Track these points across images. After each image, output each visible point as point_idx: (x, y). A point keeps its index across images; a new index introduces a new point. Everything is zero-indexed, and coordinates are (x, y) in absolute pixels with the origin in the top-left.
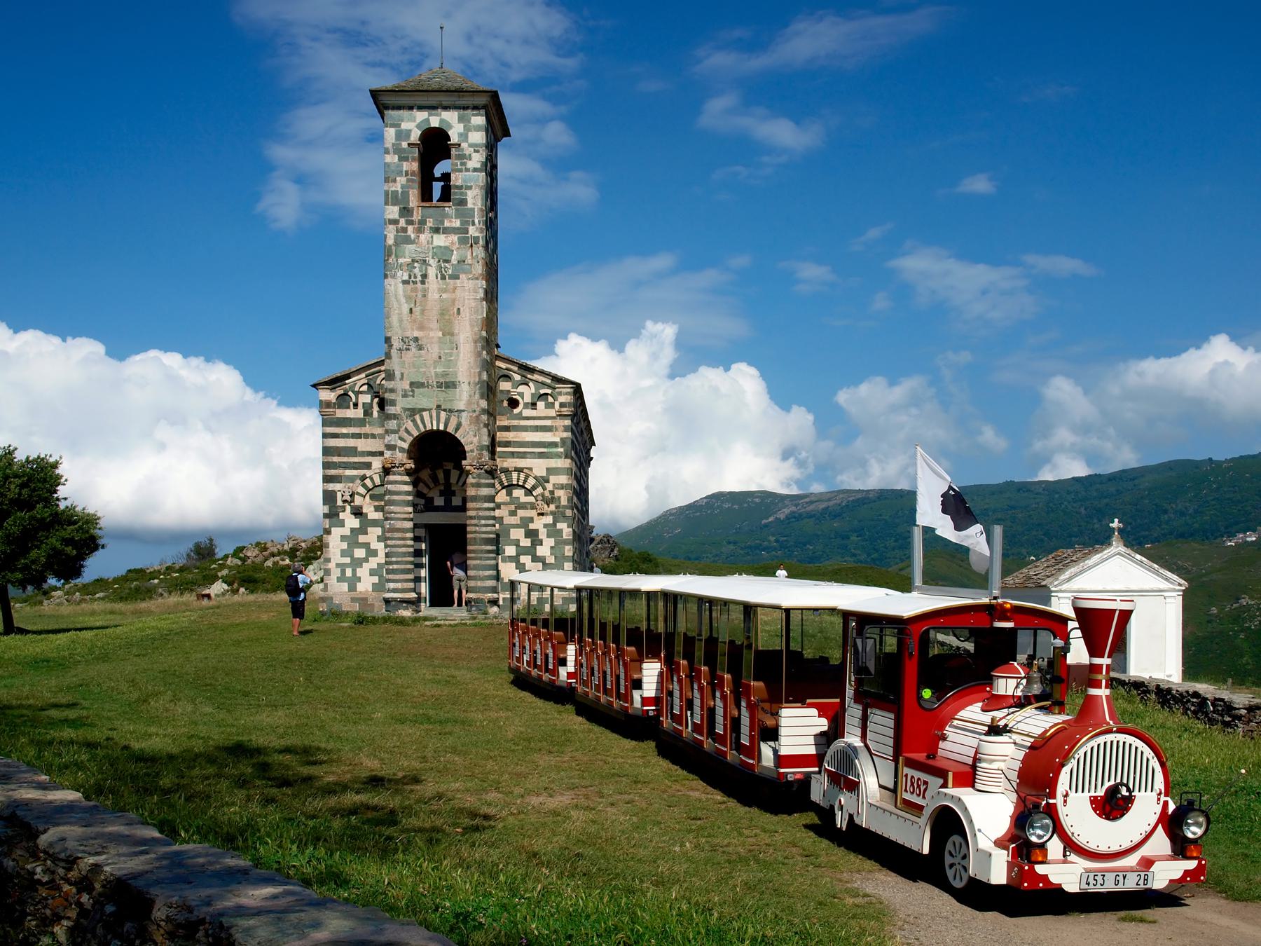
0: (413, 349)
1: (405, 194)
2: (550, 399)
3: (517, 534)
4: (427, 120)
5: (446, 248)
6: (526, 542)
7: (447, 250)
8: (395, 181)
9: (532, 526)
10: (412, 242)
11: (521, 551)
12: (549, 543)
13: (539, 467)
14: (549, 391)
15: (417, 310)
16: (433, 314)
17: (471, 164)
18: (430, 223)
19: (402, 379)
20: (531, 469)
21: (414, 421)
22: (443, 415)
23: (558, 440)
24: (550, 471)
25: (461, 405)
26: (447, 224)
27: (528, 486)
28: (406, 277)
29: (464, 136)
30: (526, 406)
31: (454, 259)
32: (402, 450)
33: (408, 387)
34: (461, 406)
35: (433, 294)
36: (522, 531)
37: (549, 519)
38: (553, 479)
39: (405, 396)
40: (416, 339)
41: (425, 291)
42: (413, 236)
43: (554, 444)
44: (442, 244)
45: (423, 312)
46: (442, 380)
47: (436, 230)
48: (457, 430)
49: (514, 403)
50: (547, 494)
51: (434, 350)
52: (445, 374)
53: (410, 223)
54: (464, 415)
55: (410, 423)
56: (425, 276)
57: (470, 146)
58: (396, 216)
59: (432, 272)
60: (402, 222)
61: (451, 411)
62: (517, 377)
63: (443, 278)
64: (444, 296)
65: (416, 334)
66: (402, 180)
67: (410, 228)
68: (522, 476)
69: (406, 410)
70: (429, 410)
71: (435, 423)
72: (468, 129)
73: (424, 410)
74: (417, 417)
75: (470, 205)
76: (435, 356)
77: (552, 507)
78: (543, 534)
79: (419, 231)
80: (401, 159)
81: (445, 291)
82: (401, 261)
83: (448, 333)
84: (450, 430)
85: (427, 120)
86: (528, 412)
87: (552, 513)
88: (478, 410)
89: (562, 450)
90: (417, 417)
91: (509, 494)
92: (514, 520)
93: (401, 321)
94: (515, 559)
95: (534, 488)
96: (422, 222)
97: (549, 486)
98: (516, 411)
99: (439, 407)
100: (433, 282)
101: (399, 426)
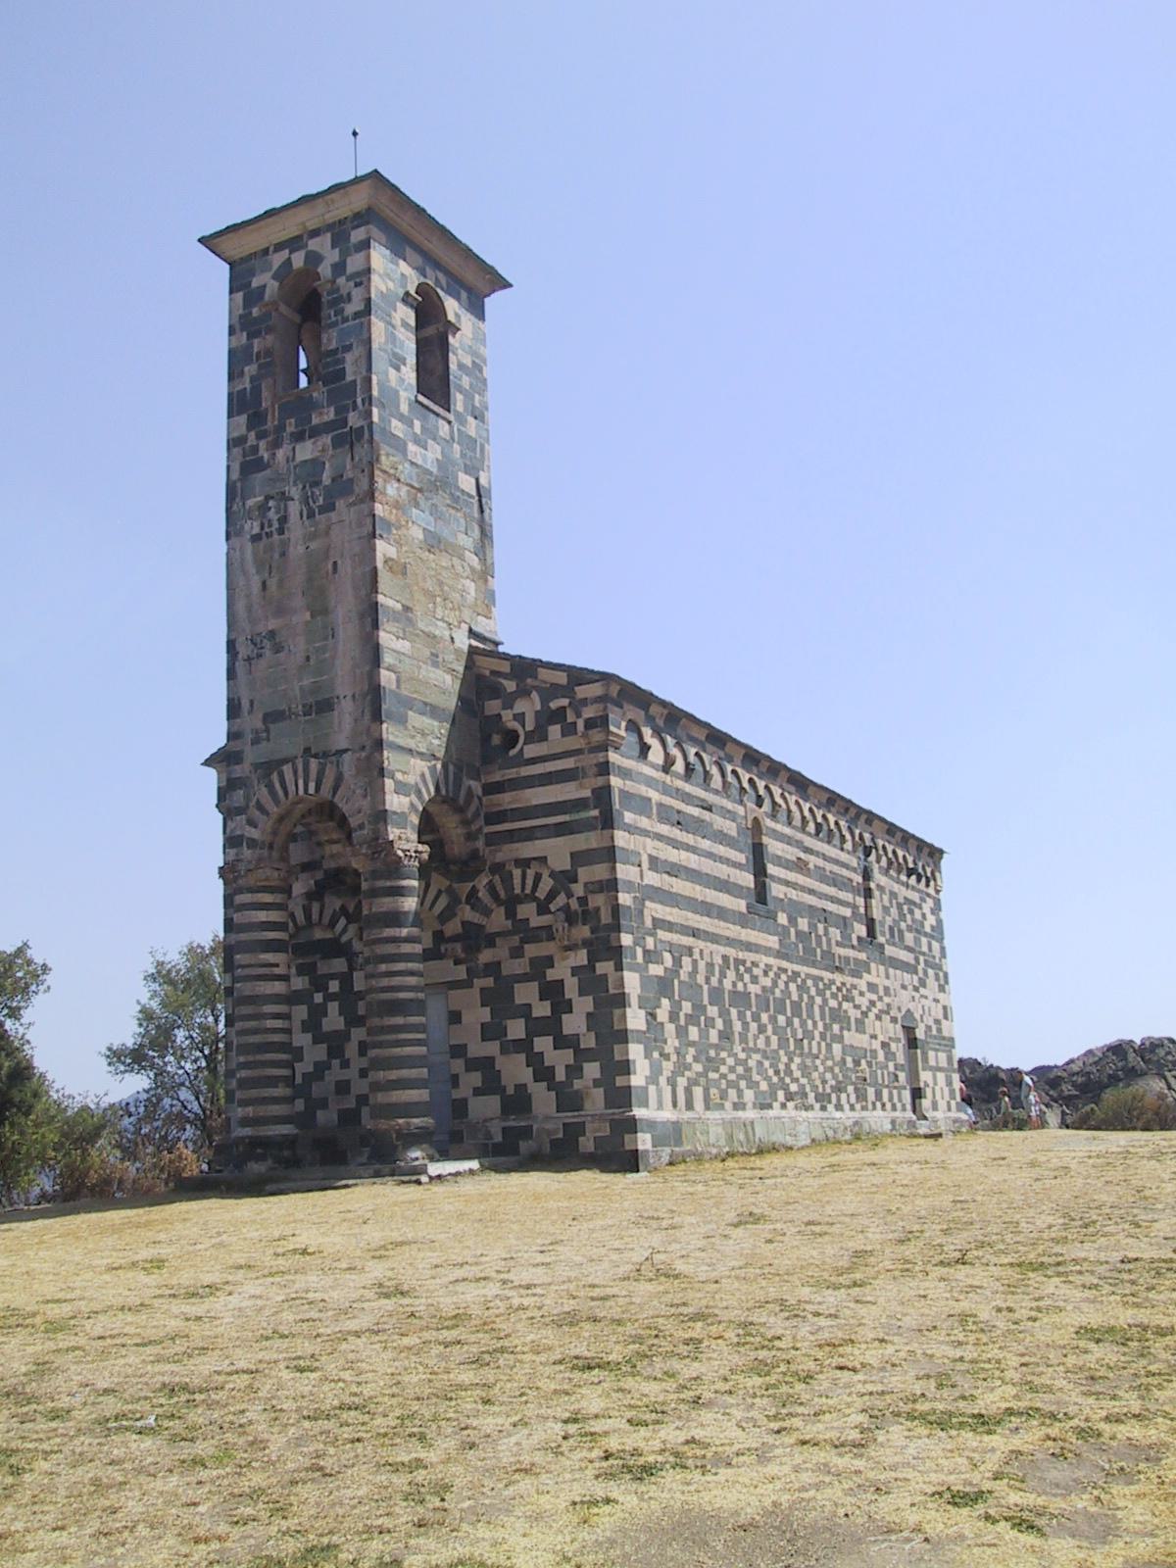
0: (267, 653)
1: (256, 390)
2: (570, 717)
3: (526, 994)
4: (288, 261)
5: (313, 461)
6: (542, 1009)
7: (316, 465)
8: (242, 374)
9: (552, 975)
10: (268, 466)
11: (536, 1027)
12: (583, 1005)
13: (557, 851)
14: (565, 702)
15: (272, 583)
16: (297, 580)
17: (350, 309)
18: (291, 426)
19: (251, 712)
20: (543, 860)
21: (270, 787)
22: (314, 764)
23: (587, 793)
24: (579, 858)
25: (342, 742)
26: (315, 420)
27: (541, 894)
28: (256, 530)
29: (339, 268)
30: (530, 738)
31: (326, 479)
32: (252, 843)
33: (259, 725)
34: (343, 745)
35: (297, 550)
36: (534, 987)
37: (581, 957)
38: (585, 874)
39: (256, 742)
40: (272, 634)
41: (285, 544)
42: (266, 456)
43: (580, 804)
44: (308, 456)
45: (281, 584)
46: (311, 700)
47: (299, 437)
48: (335, 789)
49: (511, 738)
50: (574, 905)
51: (298, 646)
52: (316, 688)
53: (259, 437)
54: (347, 757)
55: (264, 790)
56: (283, 520)
57: (349, 279)
58: (243, 430)
59: (294, 508)
60: (252, 435)
61: (325, 755)
62: (510, 686)
63: (311, 515)
64: (313, 545)
65: (273, 624)
66: (250, 370)
67: (262, 444)
68: (530, 873)
69: (256, 766)
70: (291, 760)
71: (301, 782)
72: (345, 254)
73: (285, 761)
74: (275, 777)
75: (349, 378)
76: (300, 658)
77: (584, 931)
78: (571, 988)
79: (276, 445)
80: (250, 337)
81: (313, 536)
82: (250, 503)
83: (320, 609)
84: (326, 792)
85: (288, 261)
86: (531, 751)
87: (586, 943)
88: (368, 744)
89: (595, 813)
90: (275, 777)
91: (511, 914)
92: (519, 966)
93: (249, 609)
94: (524, 1046)
95: (552, 895)
96: (281, 428)
97: (578, 889)
98: (513, 752)
99: (307, 750)
100: (296, 528)
101: (247, 798)
